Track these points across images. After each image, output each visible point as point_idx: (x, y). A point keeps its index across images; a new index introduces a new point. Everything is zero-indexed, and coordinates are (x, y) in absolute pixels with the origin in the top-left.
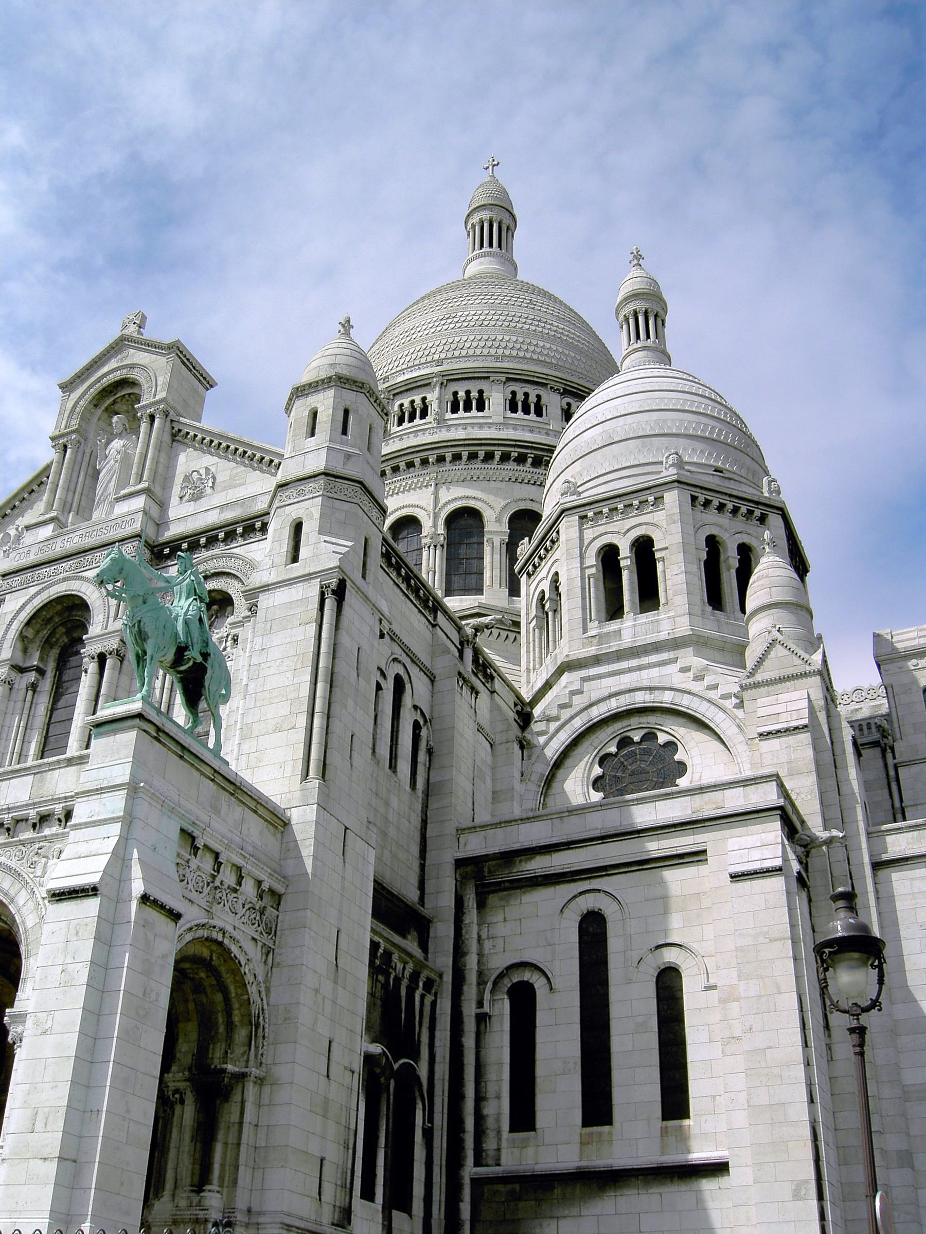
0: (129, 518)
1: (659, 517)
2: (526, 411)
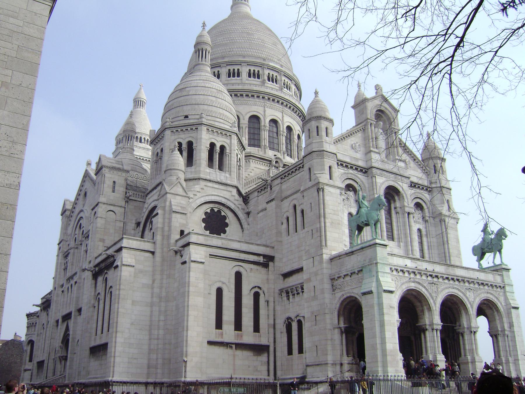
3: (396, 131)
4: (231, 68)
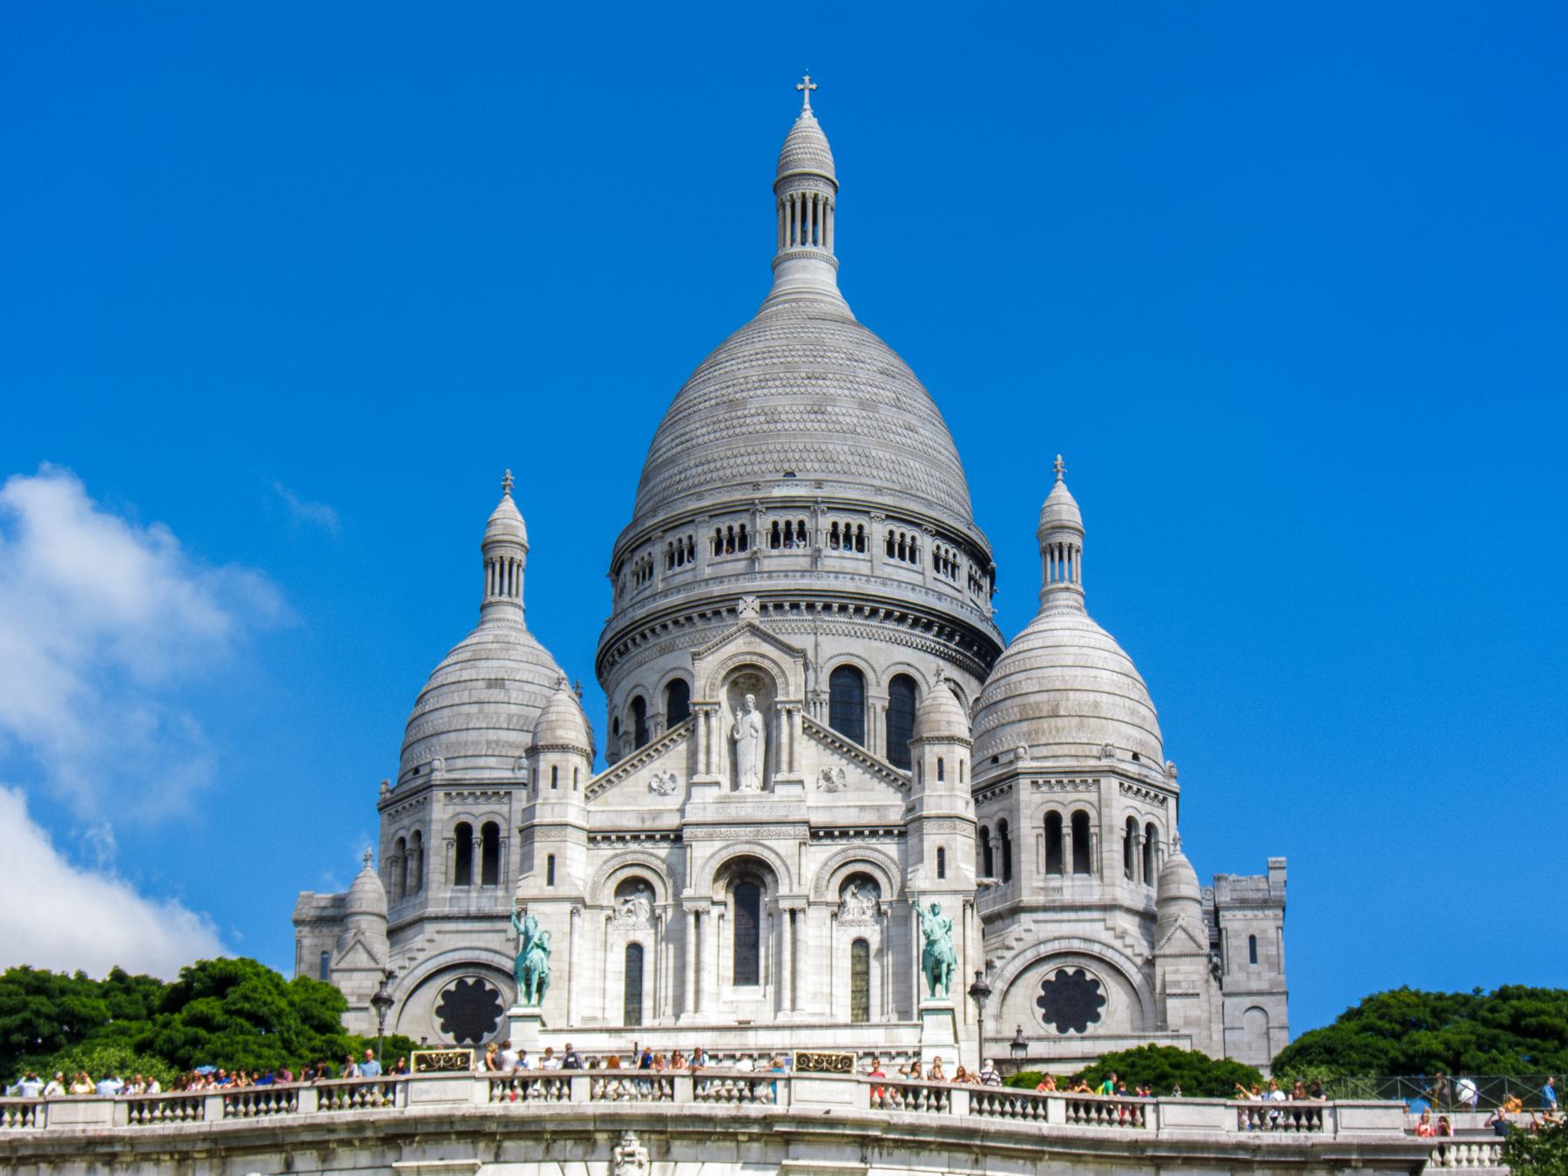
0: (795, 804)
1: (1093, 797)
2: (902, 557)
3: (788, 706)
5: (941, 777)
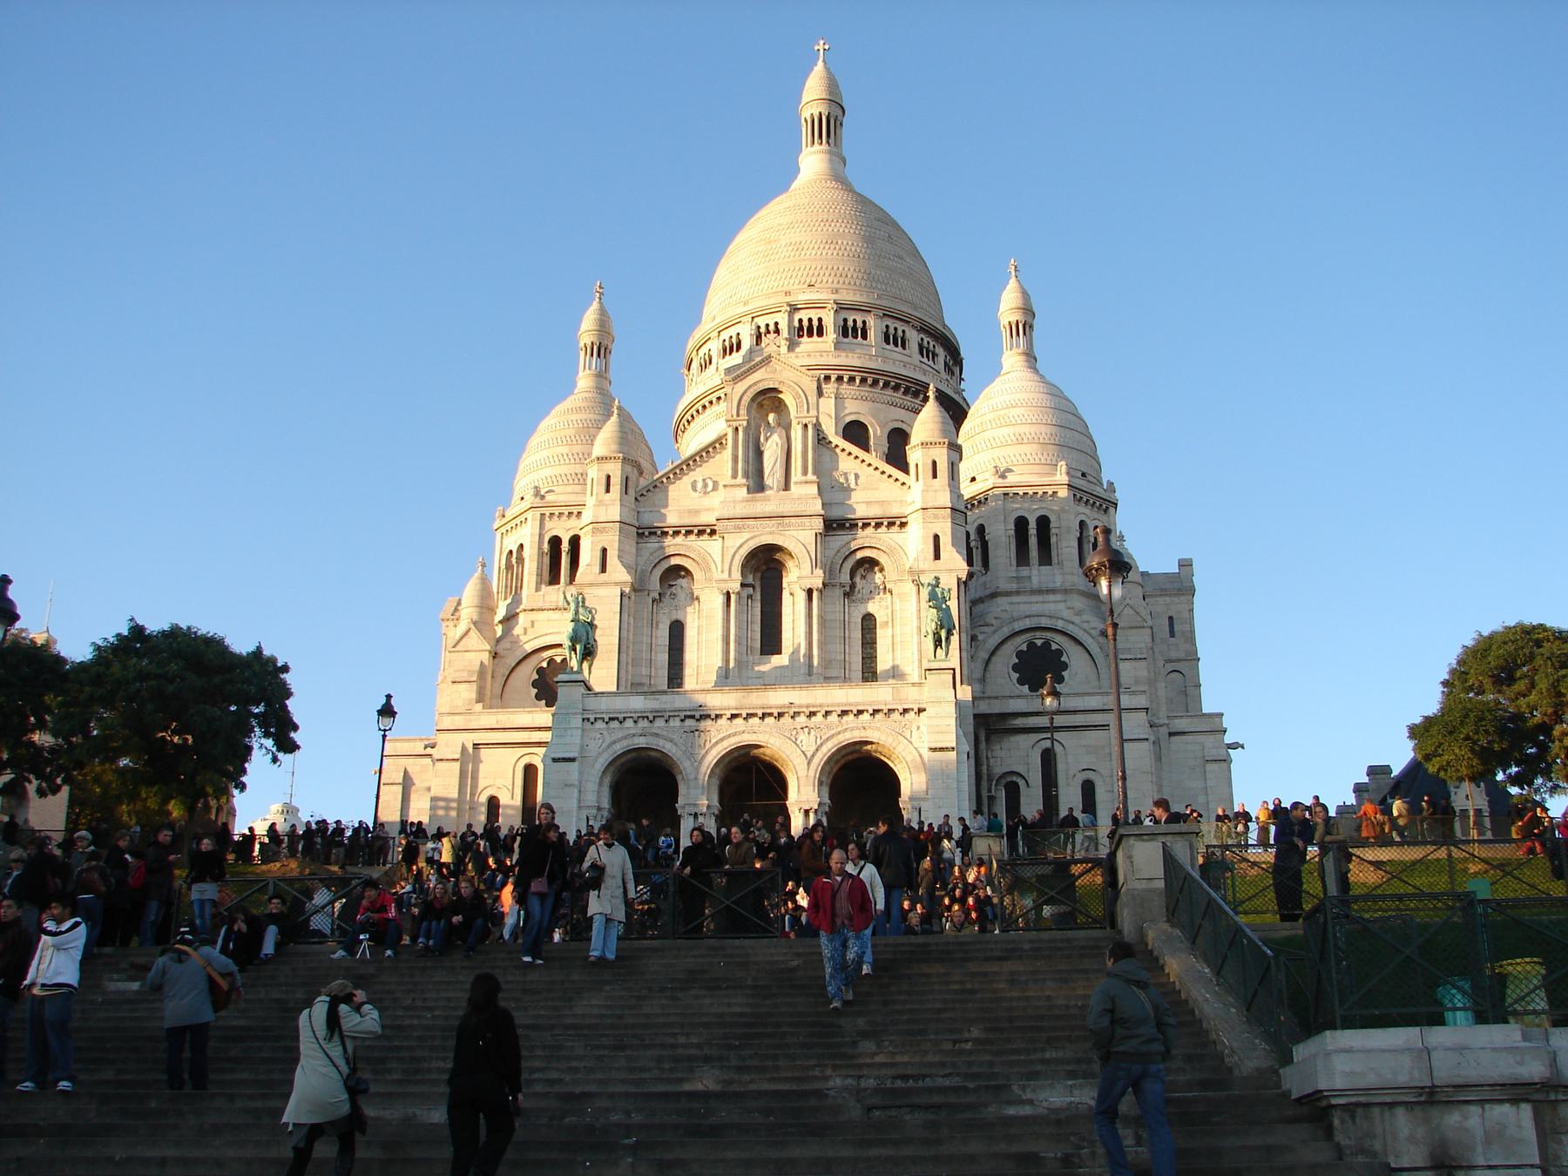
0: (811, 501)
2: (897, 346)
4: (725, 335)
5: (935, 476)
